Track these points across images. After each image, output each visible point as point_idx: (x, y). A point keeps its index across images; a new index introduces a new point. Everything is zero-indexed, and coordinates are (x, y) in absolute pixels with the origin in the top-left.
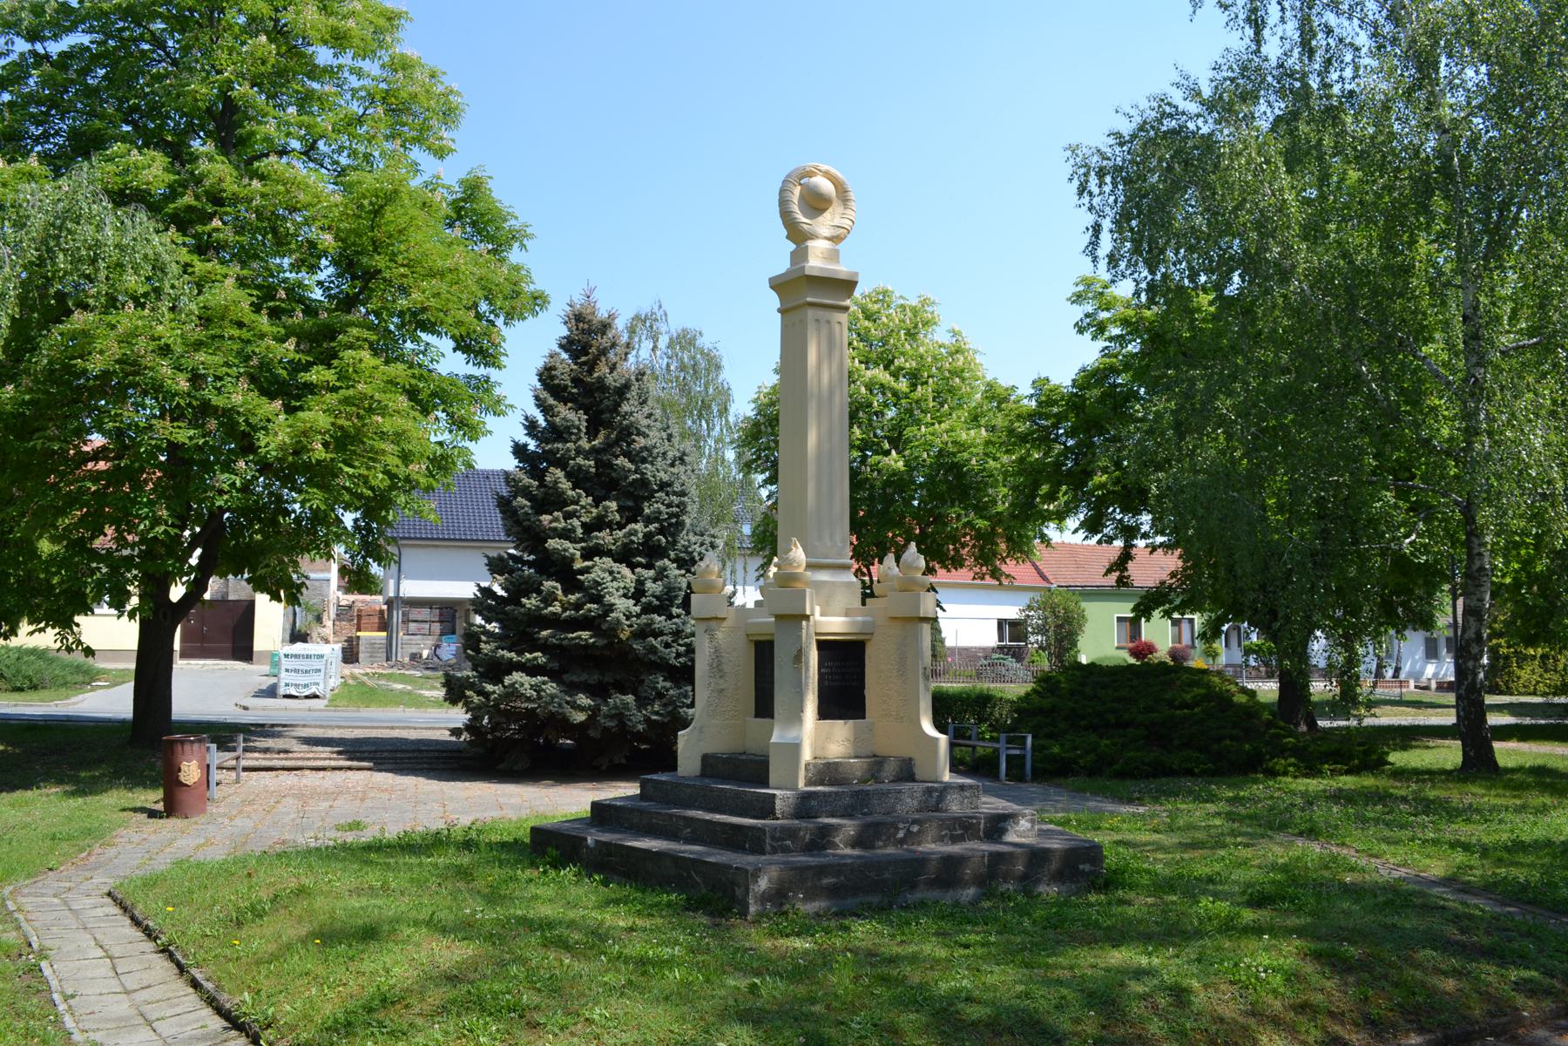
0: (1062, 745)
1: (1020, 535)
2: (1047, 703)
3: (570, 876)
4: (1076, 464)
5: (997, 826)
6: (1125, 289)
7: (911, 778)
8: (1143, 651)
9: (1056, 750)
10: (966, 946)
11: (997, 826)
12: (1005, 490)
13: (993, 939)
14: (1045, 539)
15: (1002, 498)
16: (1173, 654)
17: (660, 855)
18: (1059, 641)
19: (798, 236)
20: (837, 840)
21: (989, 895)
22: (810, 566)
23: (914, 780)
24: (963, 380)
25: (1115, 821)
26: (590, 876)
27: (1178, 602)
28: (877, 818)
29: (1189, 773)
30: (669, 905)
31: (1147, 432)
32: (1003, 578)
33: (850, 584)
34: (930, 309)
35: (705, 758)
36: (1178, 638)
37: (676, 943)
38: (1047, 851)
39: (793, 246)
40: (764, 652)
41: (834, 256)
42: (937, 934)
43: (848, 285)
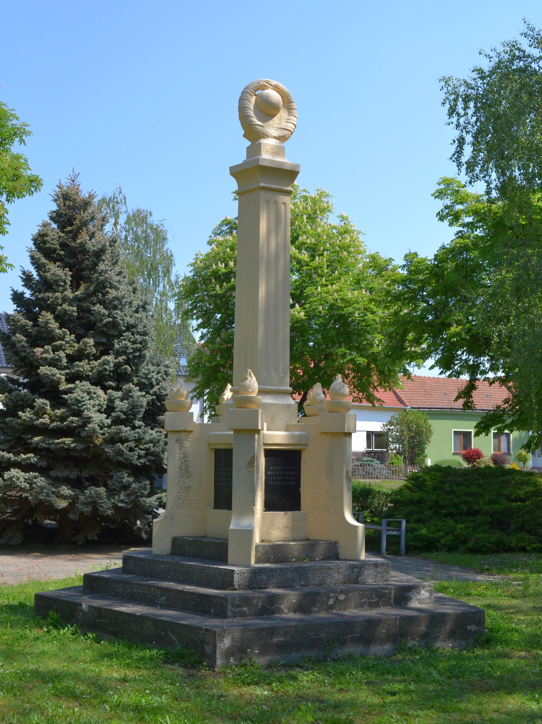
0: (428, 528)
1: (389, 370)
2: (416, 496)
3: (69, 634)
4: (437, 317)
5: (403, 595)
6: (479, 188)
7: (336, 557)
8: (472, 456)
9: (424, 532)
10: (393, 694)
11: (403, 595)
12: (380, 337)
13: (412, 687)
14: (406, 373)
15: (378, 343)
16: (495, 459)
17: (142, 618)
18: (412, 448)
19: (253, 135)
20: (282, 606)
21: (399, 650)
22: (261, 392)
23: (338, 559)
24: (349, 253)
25: (481, 590)
26: (85, 634)
27: (509, 421)
28: (312, 589)
29: (523, 550)
30: (151, 659)
31: (491, 295)
32: (375, 402)
33: (289, 406)
34: (325, 200)
35: (175, 540)
36: (498, 447)
37: (162, 692)
38: (444, 616)
39: (249, 143)
40: (223, 459)
41: (279, 151)
42: (368, 683)
43: (291, 174)
